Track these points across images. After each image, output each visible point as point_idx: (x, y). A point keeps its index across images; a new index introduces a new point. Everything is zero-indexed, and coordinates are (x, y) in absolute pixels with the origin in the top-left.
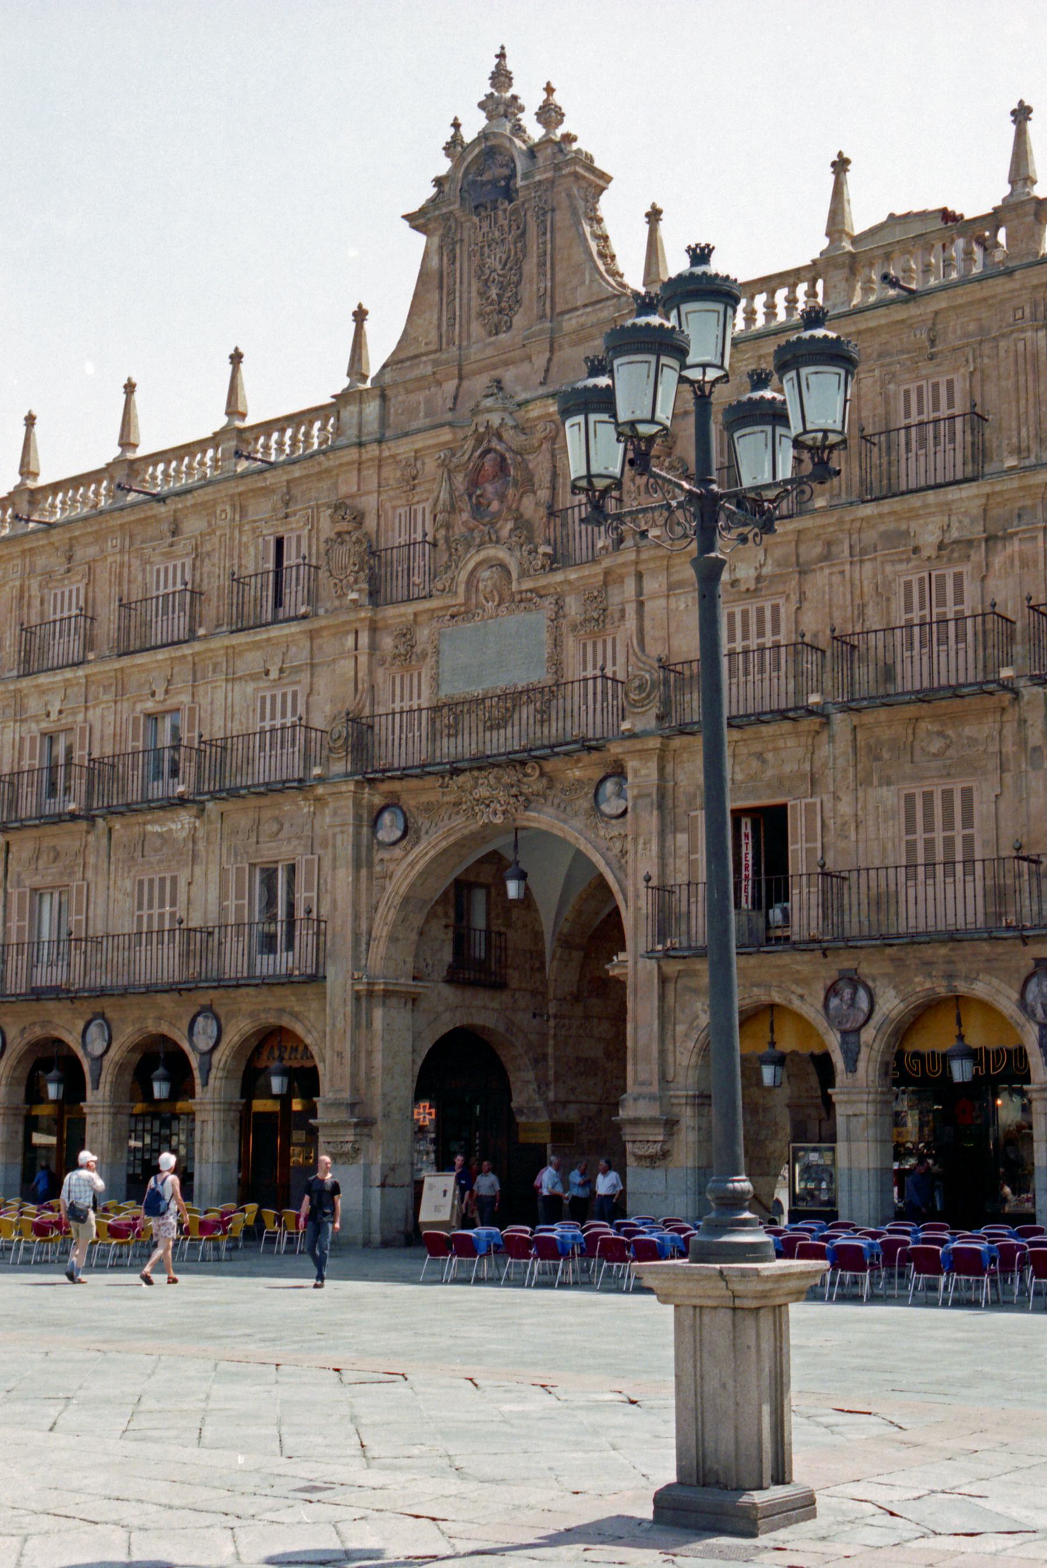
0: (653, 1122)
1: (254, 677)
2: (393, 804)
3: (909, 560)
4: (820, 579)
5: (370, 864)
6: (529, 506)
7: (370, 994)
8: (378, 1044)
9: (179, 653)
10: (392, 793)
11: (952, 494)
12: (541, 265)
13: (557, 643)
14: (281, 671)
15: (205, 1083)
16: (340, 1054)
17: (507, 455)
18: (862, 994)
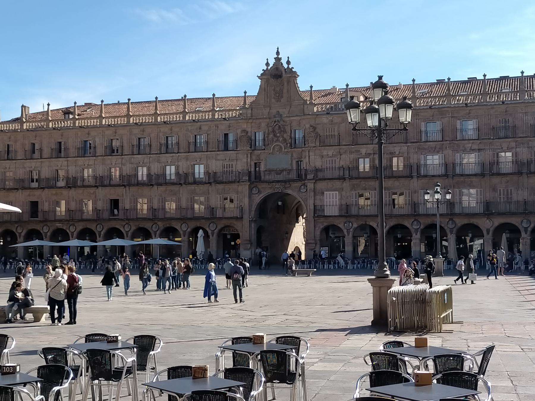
0: (313, 243)
1: (223, 160)
2: (256, 187)
3: (360, 155)
4: (343, 156)
5: (251, 197)
6: (285, 136)
7: (252, 220)
8: (253, 230)
9: (204, 154)
10: (257, 185)
11: (368, 146)
12: (288, 91)
13: (292, 161)
14: (229, 159)
15: (213, 236)
16: (246, 231)
17: (281, 126)
18: (350, 223)
